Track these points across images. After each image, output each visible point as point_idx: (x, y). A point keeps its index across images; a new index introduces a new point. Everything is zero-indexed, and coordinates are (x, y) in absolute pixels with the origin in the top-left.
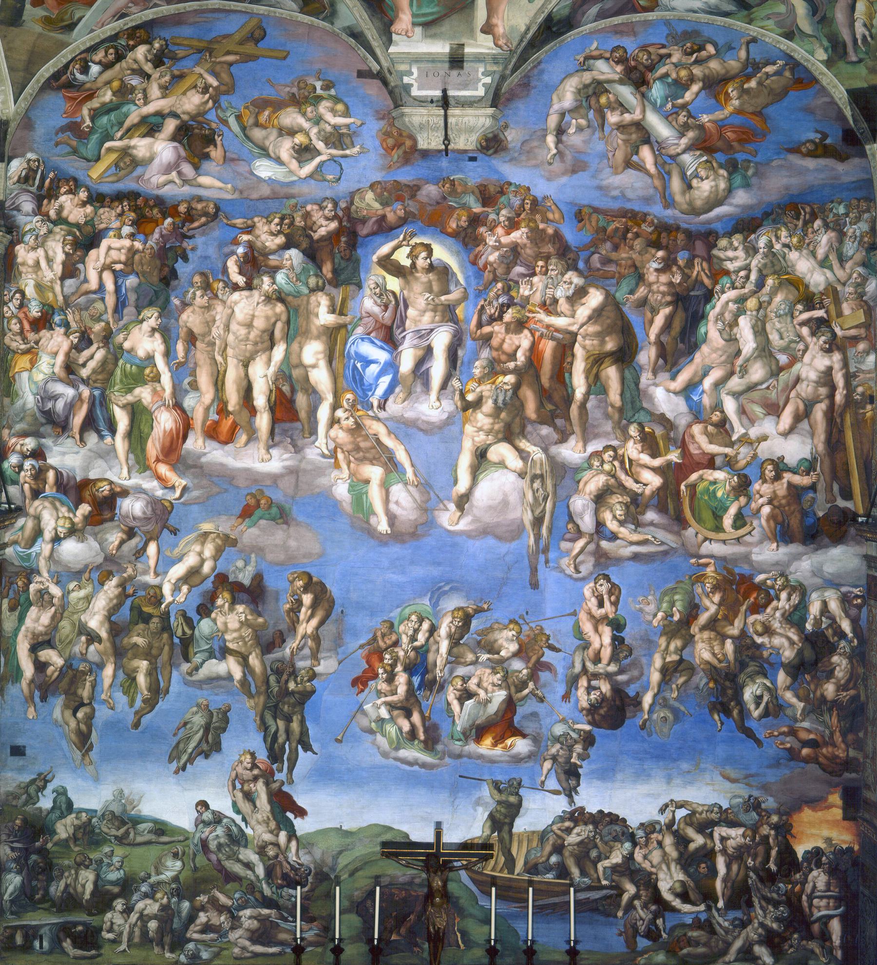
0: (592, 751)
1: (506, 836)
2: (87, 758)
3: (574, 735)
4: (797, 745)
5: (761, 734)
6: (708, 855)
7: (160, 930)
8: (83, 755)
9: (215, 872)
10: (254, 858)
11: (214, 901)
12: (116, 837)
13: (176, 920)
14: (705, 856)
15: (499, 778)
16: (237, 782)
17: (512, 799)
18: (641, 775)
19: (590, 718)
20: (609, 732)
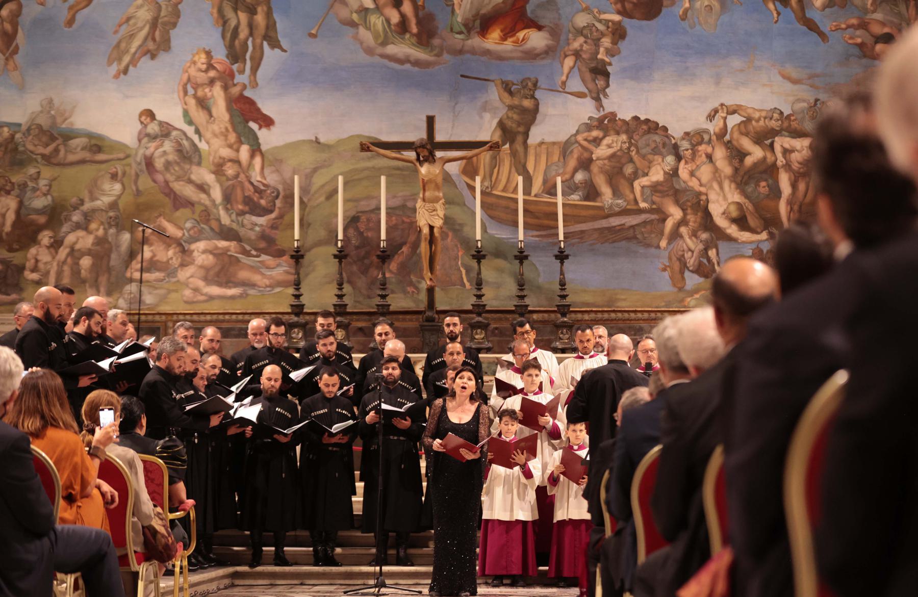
0: (622, 45)
1: (519, 148)
2: (11, 63)
3: (601, 27)
4: (869, 40)
5: (826, 26)
6: (769, 171)
7: (96, 269)
8: (7, 59)
9: (161, 197)
10: (210, 178)
11: (161, 234)
12: (43, 156)
13: (114, 256)
14: (765, 172)
15: (510, 77)
16: (188, 86)
17: (527, 103)
18: (685, 75)
19: (619, 6)
20: (644, 23)
